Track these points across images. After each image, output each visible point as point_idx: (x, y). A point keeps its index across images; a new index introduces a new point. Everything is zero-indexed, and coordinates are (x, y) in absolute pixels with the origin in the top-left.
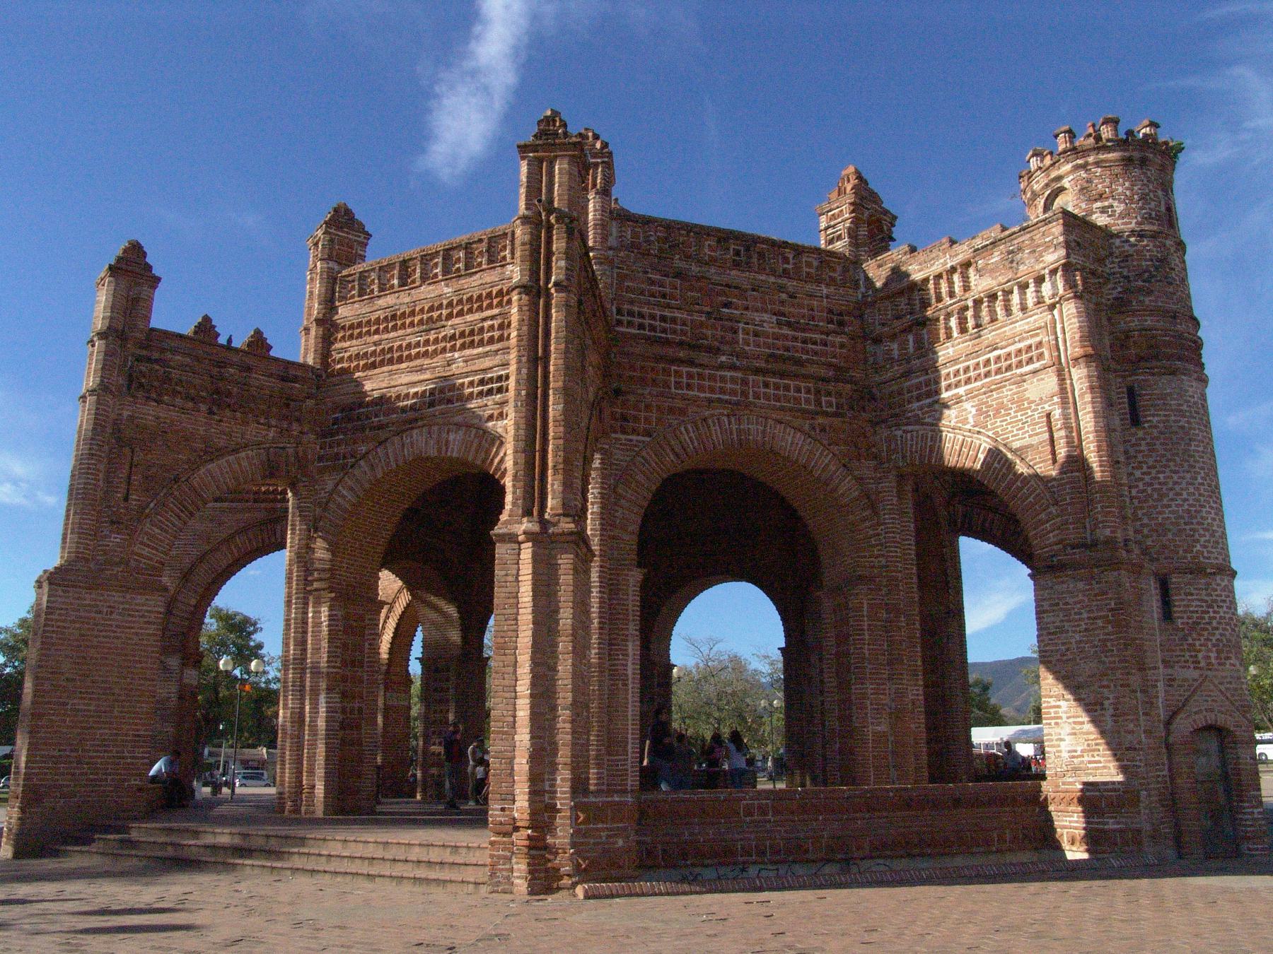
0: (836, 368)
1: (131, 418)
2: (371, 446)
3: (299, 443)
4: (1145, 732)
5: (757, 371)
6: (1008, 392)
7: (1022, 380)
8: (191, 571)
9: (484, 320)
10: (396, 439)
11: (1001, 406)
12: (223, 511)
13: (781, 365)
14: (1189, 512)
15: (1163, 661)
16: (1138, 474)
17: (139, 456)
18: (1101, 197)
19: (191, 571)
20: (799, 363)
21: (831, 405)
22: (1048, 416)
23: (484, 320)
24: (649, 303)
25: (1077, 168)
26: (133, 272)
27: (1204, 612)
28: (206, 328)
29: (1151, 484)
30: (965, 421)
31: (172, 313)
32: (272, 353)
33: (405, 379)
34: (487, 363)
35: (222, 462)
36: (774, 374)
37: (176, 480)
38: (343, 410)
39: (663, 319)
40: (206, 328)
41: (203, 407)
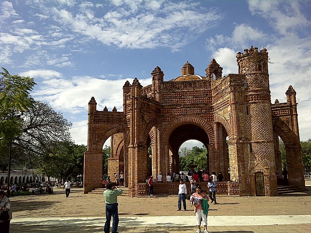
0: (206, 104)
1: (95, 126)
3: (123, 126)
4: (242, 173)
5: (188, 108)
13: (194, 105)
14: (257, 131)
15: (250, 160)
16: (247, 123)
17: (97, 132)
18: (244, 67)
20: (197, 104)
21: (204, 111)
24: (168, 98)
26: (93, 103)
27: (258, 150)
28: (106, 109)
29: (249, 126)
31: (100, 108)
32: (117, 111)
35: (110, 131)
36: (192, 107)
37: (103, 135)
39: (171, 101)
40: (106, 109)
41: (106, 123)
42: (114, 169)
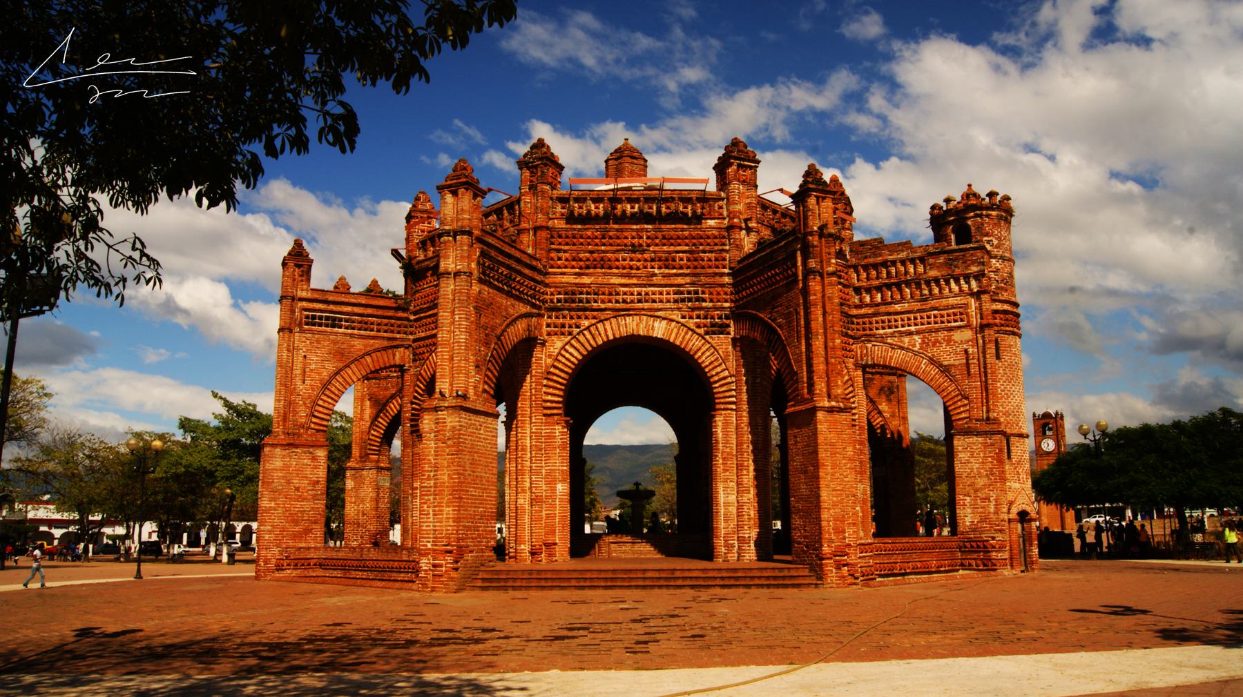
2: (594, 321)
6: (941, 335)
7: (950, 329)
8: (329, 382)
10: (613, 321)
11: (937, 341)
12: (352, 335)
18: (987, 235)
19: (329, 382)
22: (966, 351)
25: (976, 216)
30: (914, 345)
33: (615, 280)
34: (680, 280)
38: (566, 293)
42: (297, 489)
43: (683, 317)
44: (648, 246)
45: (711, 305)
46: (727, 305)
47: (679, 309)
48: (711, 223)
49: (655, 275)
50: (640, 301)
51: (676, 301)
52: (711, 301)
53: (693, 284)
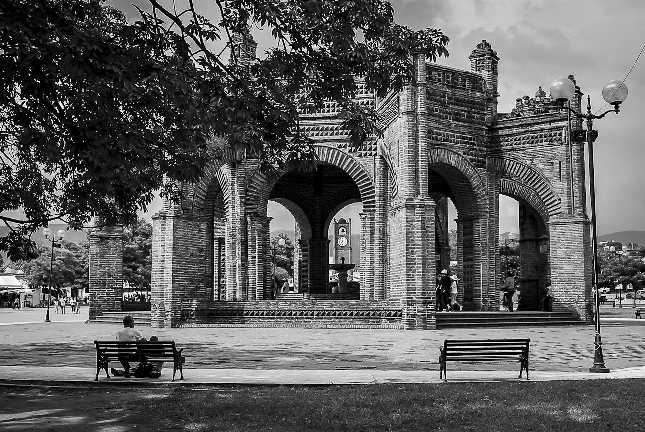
9: (462, 111)
23: (462, 111)
34: (463, 130)
42: (191, 254)
43: (465, 154)
44: (448, 104)
45: (478, 148)
46: (485, 149)
47: (463, 148)
48: (478, 94)
49: (451, 124)
50: (444, 140)
51: (461, 143)
52: (478, 146)
53: (470, 133)
